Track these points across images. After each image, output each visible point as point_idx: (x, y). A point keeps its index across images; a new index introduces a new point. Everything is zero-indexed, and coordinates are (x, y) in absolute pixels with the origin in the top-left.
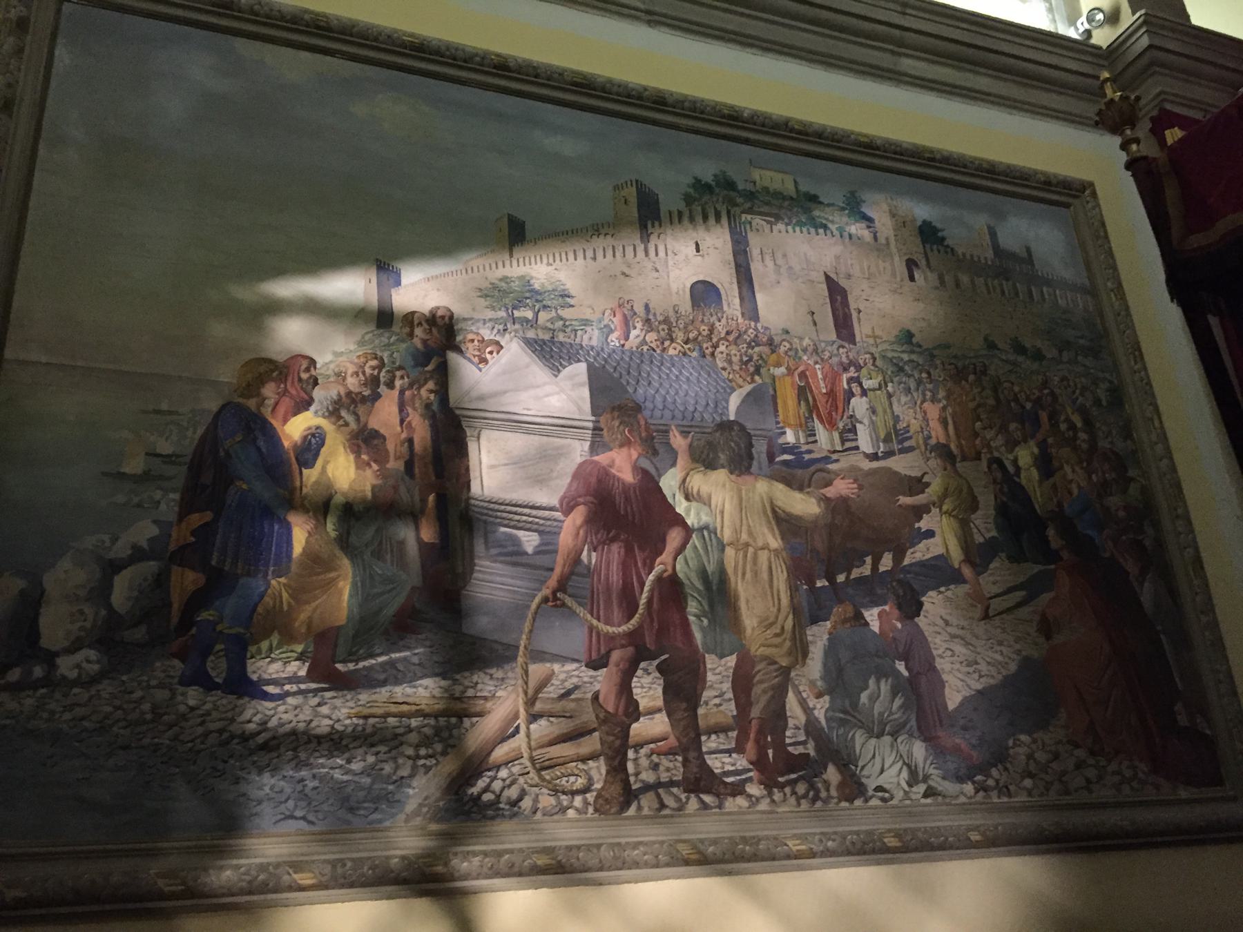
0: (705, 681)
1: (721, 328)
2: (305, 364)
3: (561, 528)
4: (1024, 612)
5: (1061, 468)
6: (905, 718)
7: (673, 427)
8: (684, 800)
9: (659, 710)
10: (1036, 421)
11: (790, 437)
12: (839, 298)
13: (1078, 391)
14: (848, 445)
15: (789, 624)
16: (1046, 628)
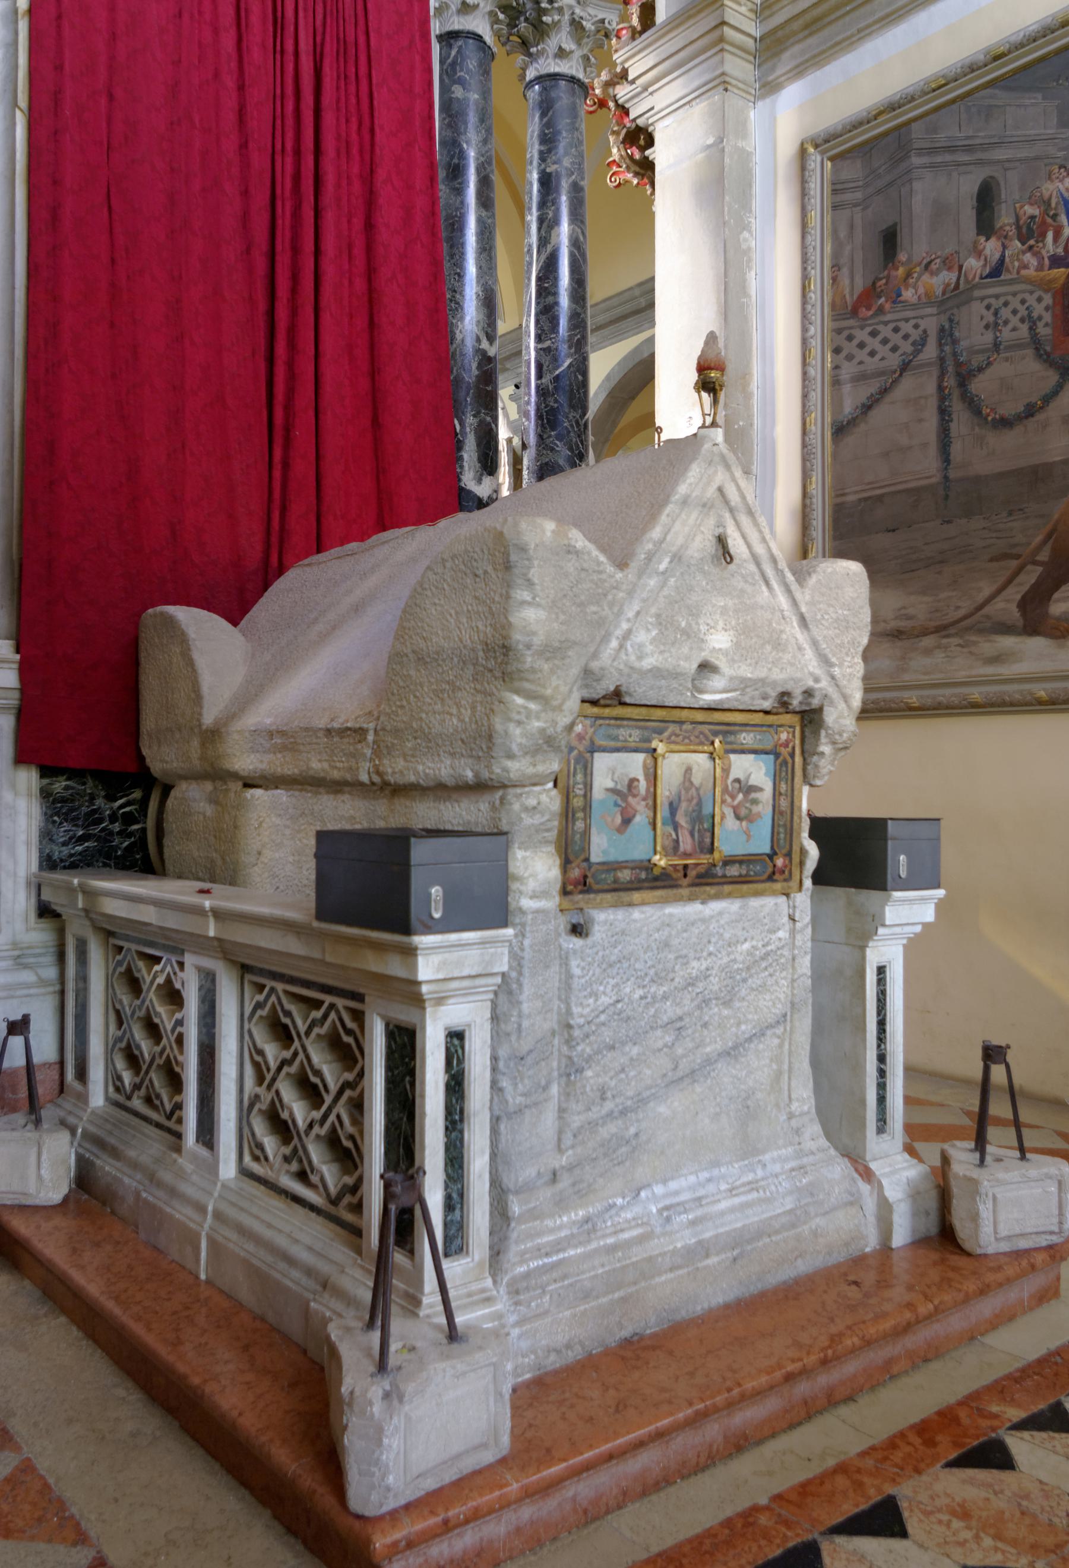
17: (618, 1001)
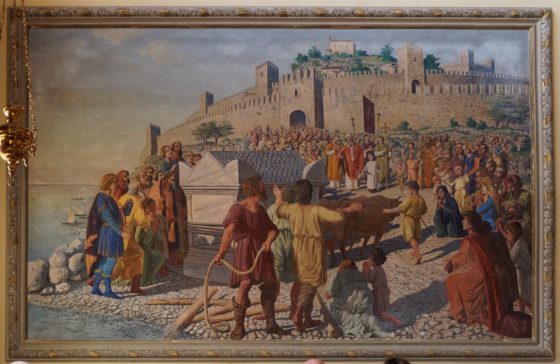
0: (279, 292)
1: (303, 134)
2: (125, 174)
3: (223, 233)
4: (439, 261)
5: (482, 187)
6: (367, 307)
7: (275, 186)
8: (266, 336)
9: (259, 303)
10: (472, 164)
11: (332, 185)
12: (369, 109)
13: (503, 145)
14: (361, 186)
15: (319, 269)
16: (450, 268)
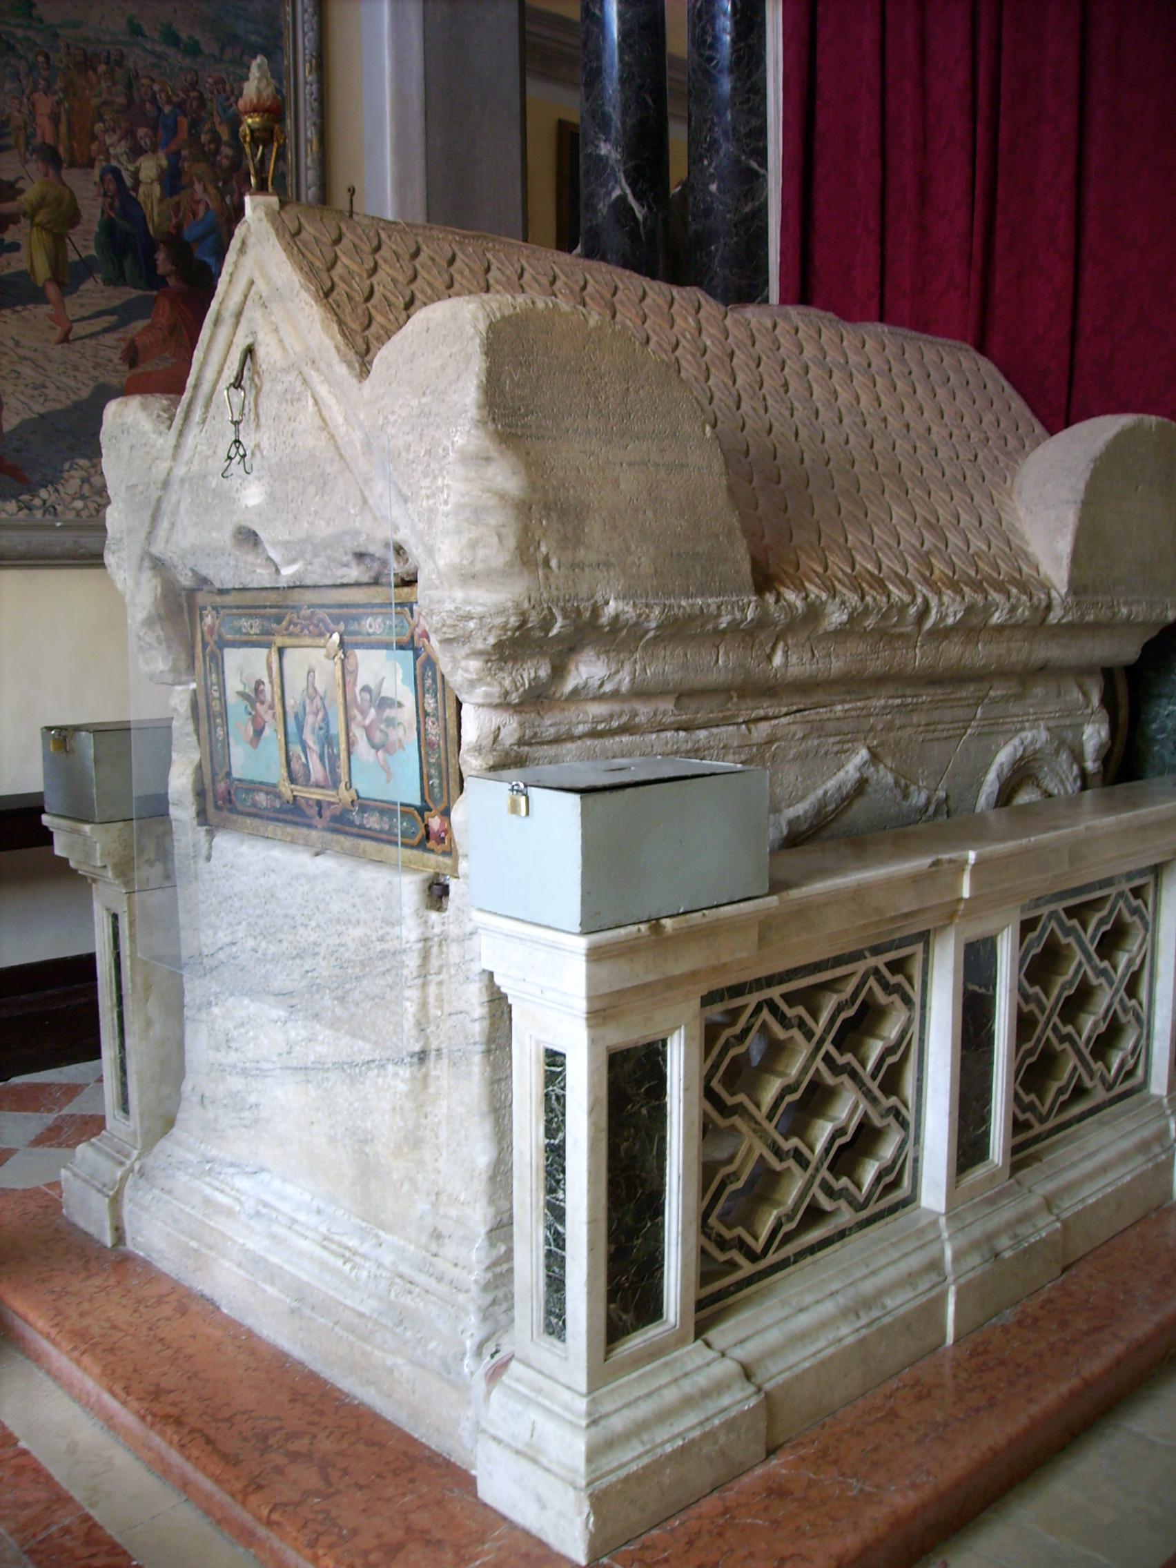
4: (109, 339)
5: (192, 183)
10: (175, 131)
17: (234, 944)
